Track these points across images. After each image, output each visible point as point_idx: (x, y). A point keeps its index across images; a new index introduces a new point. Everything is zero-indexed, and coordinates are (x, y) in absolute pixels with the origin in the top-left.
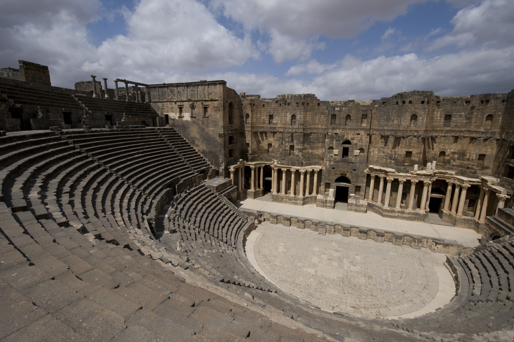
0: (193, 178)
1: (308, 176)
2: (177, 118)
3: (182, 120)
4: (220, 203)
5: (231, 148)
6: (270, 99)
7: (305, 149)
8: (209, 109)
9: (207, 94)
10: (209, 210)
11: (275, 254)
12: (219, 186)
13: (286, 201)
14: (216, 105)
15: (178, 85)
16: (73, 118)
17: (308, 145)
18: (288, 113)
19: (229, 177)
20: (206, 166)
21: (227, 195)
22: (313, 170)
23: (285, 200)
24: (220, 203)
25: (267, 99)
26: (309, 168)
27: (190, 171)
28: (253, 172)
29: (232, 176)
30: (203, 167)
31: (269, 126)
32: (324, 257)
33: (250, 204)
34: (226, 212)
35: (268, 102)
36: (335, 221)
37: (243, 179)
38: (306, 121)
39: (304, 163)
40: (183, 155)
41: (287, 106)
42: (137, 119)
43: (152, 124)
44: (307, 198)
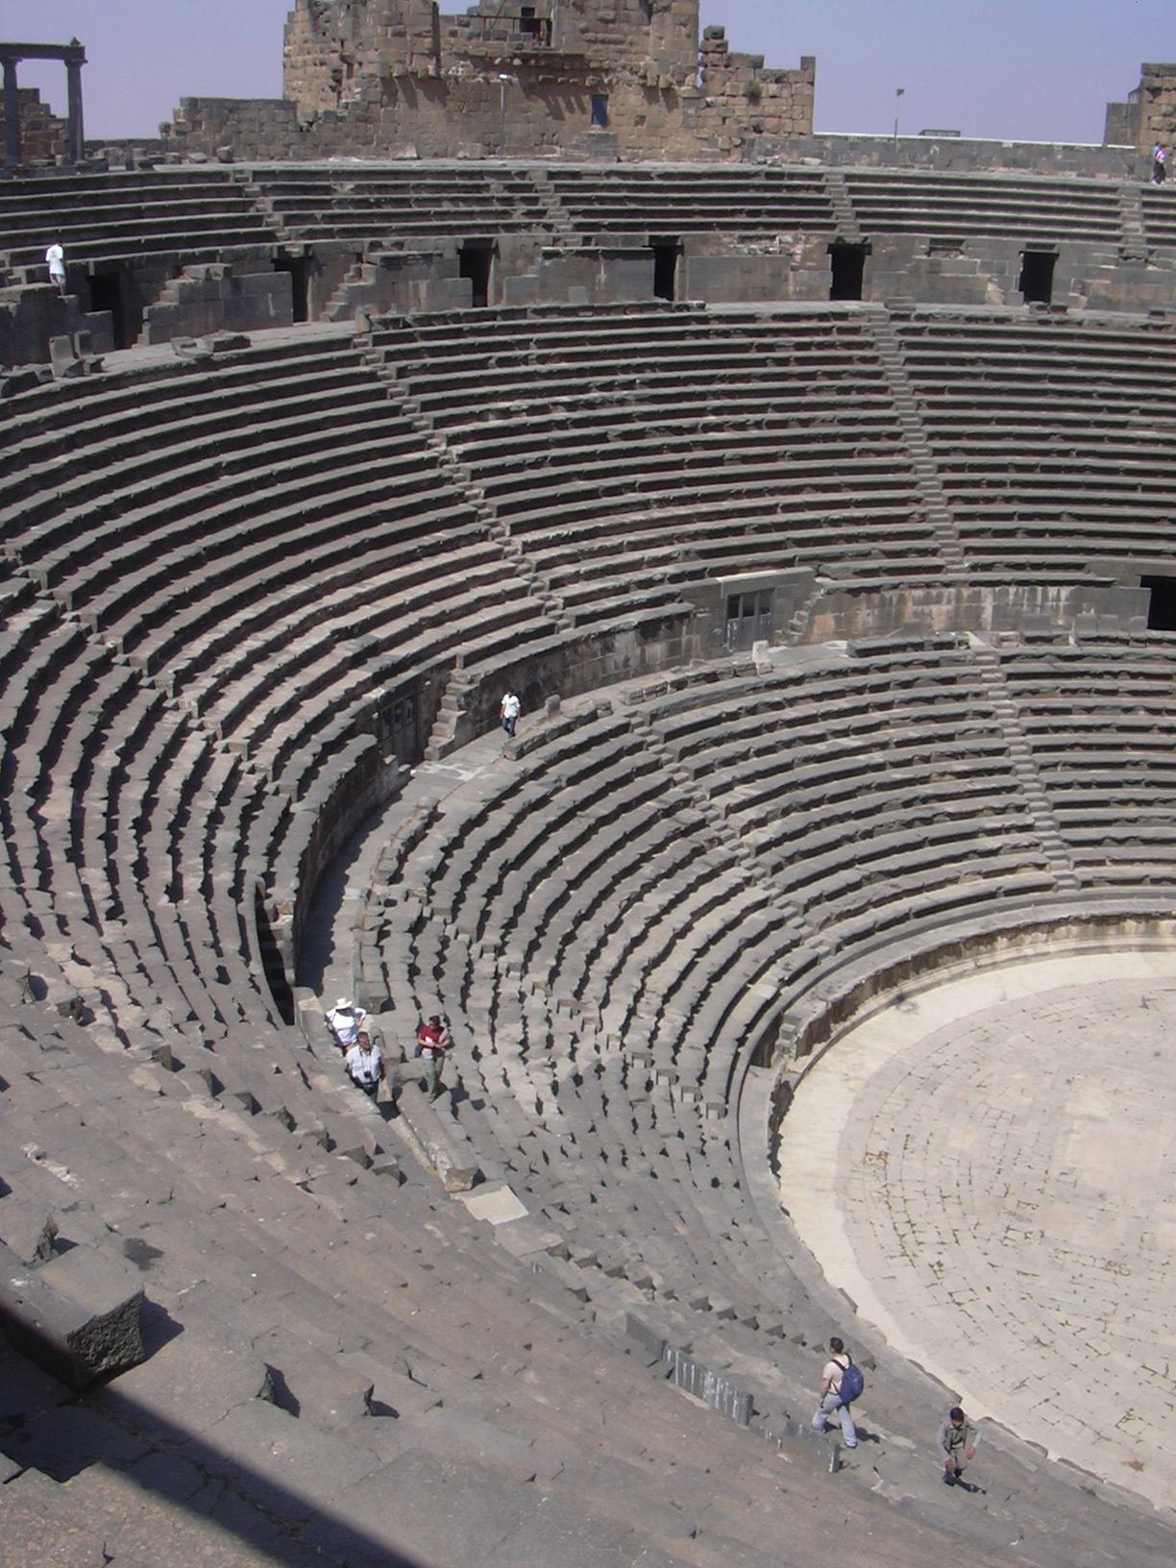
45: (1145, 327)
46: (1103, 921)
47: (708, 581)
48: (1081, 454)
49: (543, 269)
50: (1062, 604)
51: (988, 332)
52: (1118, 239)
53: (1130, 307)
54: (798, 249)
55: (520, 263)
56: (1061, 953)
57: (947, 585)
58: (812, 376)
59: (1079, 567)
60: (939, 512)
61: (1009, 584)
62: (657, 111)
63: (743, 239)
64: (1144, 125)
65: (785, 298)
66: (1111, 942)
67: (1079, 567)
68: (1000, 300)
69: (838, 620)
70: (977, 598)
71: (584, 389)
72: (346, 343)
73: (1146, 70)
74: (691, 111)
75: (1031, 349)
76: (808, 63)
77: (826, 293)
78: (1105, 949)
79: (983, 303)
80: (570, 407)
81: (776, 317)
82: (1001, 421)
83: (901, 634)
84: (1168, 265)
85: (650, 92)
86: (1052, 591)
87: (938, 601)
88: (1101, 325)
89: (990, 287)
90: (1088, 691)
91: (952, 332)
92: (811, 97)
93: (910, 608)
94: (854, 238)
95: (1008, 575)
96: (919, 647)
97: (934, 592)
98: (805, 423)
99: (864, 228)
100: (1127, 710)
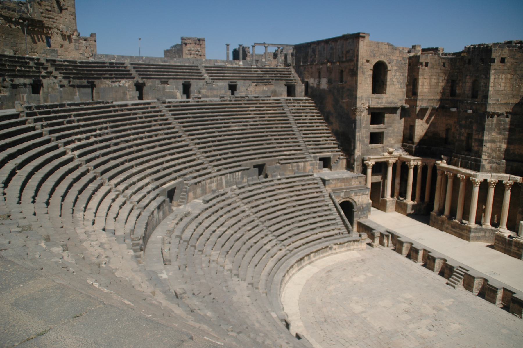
0: (302, 164)
1: (492, 191)
2: (315, 86)
3: (319, 88)
4: (323, 201)
5: (377, 131)
6: (454, 54)
7: (493, 141)
8: (345, 74)
9: (344, 52)
10: (295, 204)
11: (344, 280)
12: (333, 180)
13: (447, 228)
14: (352, 68)
15: (318, 43)
16: (193, 89)
17: (500, 134)
18: (468, 77)
19: (364, 172)
20: (332, 152)
21: (342, 194)
22: (500, 182)
23: (446, 225)
24: (323, 201)
25: (450, 54)
26: (492, 178)
27: (302, 154)
28: (411, 172)
29: (369, 171)
30: (328, 152)
31: (450, 98)
32: (405, 306)
33: (389, 219)
34: (320, 214)
35: (451, 59)
36: (487, 274)
37: (398, 181)
38: (497, 92)
39: (487, 166)
40: (304, 134)
41: (466, 65)
42: (265, 88)
43: (285, 93)
44: (486, 230)
45: (221, 101)
46: (301, 260)
47: (161, 189)
48: (225, 135)
49: (61, 92)
50: (240, 177)
51: (184, 106)
52: (204, 79)
53: (212, 97)
54: (127, 85)
55: (50, 90)
56: (296, 272)
57: (215, 177)
58: (150, 122)
59: (240, 166)
60: (201, 157)
61: (227, 173)
62: (66, 43)
63: (113, 82)
64: (184, 53)
65: (127, 100)
66: (303, 264)
67: (240, 166)
68: (180, 97)
69: (193, 193)
70: (221, 179)
71: (95, 130)
72: (17, 116)
73: (182, 38)
74: (77, 44)
75: (198, 109)
76: (93, 35)
77: (137, 98)
78: (303, 267)
79: (176, 98)
80: (95, 136)
81: (133, 105)
82: (202, 129)
83: (213, 193)
84: (218, 85)
85: (64, 37)
86: (237, 173)
87: (213, 182)
88: (211, 101)
89: (178, 94)
90: (260, 199)
91: (178, 106)
92: (96, 46)
93: (208, 186)
94: (141, 81)
95: (227, 171)
96: (218, 196)
97: (212, 180)
98: (156, 135)
99: (142, 78)
100: (271, 201)
